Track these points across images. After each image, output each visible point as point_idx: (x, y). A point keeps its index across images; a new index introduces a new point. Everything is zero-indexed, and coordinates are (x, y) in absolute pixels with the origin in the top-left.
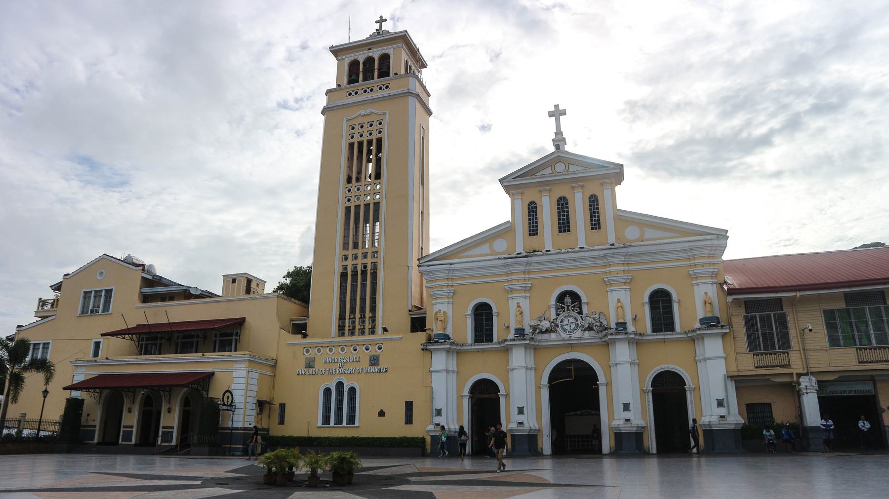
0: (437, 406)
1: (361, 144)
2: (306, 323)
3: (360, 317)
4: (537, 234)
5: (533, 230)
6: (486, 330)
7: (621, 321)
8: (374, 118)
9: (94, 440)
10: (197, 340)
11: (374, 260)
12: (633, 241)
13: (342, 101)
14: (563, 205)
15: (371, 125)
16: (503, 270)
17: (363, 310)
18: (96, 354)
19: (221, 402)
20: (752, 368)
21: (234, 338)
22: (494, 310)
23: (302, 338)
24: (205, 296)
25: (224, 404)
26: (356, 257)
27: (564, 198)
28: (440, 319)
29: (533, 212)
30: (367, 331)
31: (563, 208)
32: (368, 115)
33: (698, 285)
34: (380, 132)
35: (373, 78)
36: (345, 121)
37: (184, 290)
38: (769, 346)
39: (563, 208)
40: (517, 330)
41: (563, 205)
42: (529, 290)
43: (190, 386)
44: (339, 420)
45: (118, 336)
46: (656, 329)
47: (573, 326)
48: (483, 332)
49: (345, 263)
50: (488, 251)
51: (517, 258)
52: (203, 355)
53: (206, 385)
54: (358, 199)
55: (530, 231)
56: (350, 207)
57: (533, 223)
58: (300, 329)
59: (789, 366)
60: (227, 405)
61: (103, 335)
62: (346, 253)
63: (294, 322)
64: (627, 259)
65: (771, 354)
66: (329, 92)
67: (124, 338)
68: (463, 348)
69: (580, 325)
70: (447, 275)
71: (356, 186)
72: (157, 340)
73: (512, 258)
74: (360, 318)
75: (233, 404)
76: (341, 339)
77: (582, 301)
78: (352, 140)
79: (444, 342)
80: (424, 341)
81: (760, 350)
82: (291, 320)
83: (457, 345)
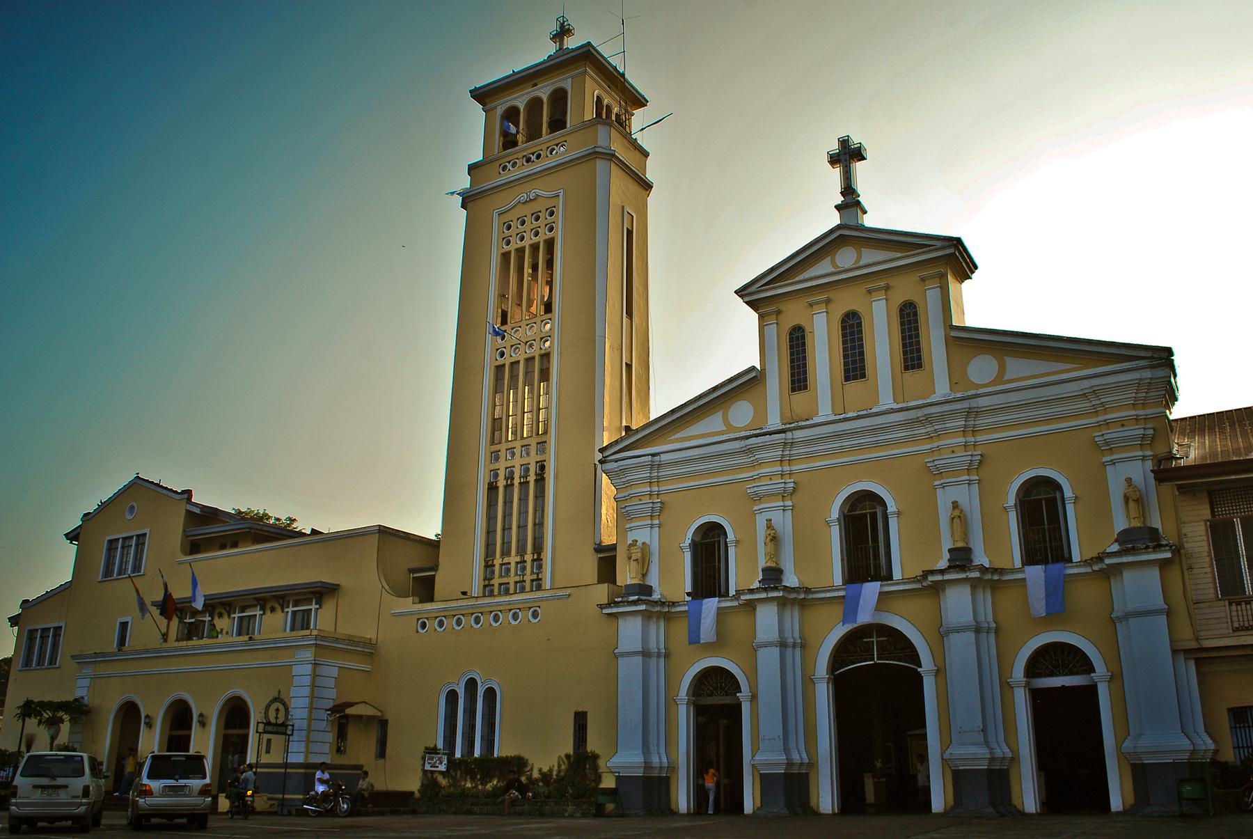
5: (799, 381)
7: (960, 545)
12: (985, 386)
14: (852, 328)
15: (537, 219)
16: (745, 459)
20: (1225, 632)
24: (279, 536)
28: (634, 557)
33: (1114, 463)
41: (852, 328)
42: (792, 494)
50: (723, 428)
55: (793, 382)
63: (415, 575)
64: (972, 423)
66: (472, 168)
82: (412, 571)
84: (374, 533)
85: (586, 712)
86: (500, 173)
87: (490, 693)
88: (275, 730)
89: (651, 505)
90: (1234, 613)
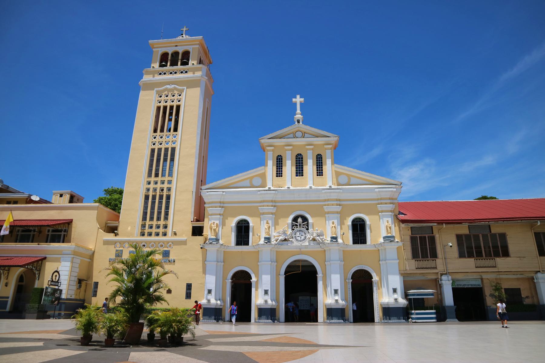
7: (334, 236)
10: (34, 233)
11: (169, 186)
21: (63, 233)
23: (114, 236)
27: (300, 154)
29: (279, 161)
31: (299, 161)
38: (425, 256)
39: (299, 161)
40: (265, 238)
46: (355, 242)
47: (303, 238)
49: (148, 186)
52: (38, 245)
53: (39, 267)
56: (155, 149)
58: (113, 230)
59: (436, 268)
62: (149, 179)
65: (425, 261)
69: (307, 237)
75: (59, 281)
77: (309, 221)
80: (202, 243)
81: (419, 258)
85: (191, 284)
88: (54, 284)
90: (416, 264)
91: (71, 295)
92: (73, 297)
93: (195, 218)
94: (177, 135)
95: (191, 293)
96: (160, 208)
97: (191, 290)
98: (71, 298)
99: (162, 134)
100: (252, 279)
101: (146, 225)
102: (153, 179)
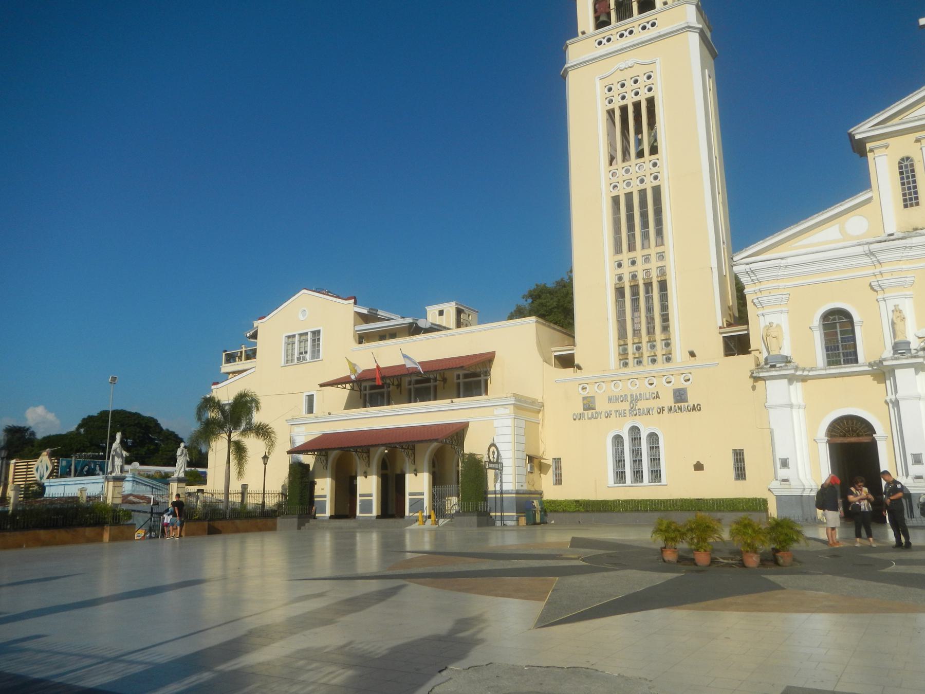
0: (780, 454)
1: (624, 109)
2: (573, 354)
3: (648, 340)
4: (917, 204)
6: (844, 347)
8: (640, 71)
9: (325, 513)
10: (435, 383)
11: (660, 264)
13: (593, 54)
15: (636, 82)
16: (867, 260)
17: (651, 331)
18: (310, 410)
19: (485, 459)
21: (482, 378)
22: (856, 318)
25: (490, 462)
26: (633, 263)
30: (659, 358)
32: (630, 67)
34: (650, 90)
35: (631, 15)
36: (598, 82)
37: (409, 323)
43: (444, 441)
44: (638, 475)
45: (339, 386)
48: (838, 350)
49: (619, 271)
51: (889, 241)
52: (452, 402)
54: (628, 184)
55: (905, 200)
57: (909, 188)
58: (567, 362)
60: (493, 463)
61: (322, 385)
62: (619, 257)
67: (345, 388)
68: (811, 373)
70: (776, 274)
71: (623, 168)
72: (430, 382)
73: (880, 242)
74: (647, 342)
75: (499, 461)
76: (625, 370)
78: (610, 106)
79: (784, 366)
80: (753, 367)
83: (804, 370)
84: (533, 323)
86: (596, 47)
87: (653, 437)
89: (781, 296)
91: (522, 484)
92: (525, 488)
93: (724, 320)
94: (658, 159)
95: (744, 468)
96: (649, 309)
97: (744, 462)
98: (522, 488)
99: (626, 164)
100: (875, 433)
101: (627, 344)
102: (625, 256)
